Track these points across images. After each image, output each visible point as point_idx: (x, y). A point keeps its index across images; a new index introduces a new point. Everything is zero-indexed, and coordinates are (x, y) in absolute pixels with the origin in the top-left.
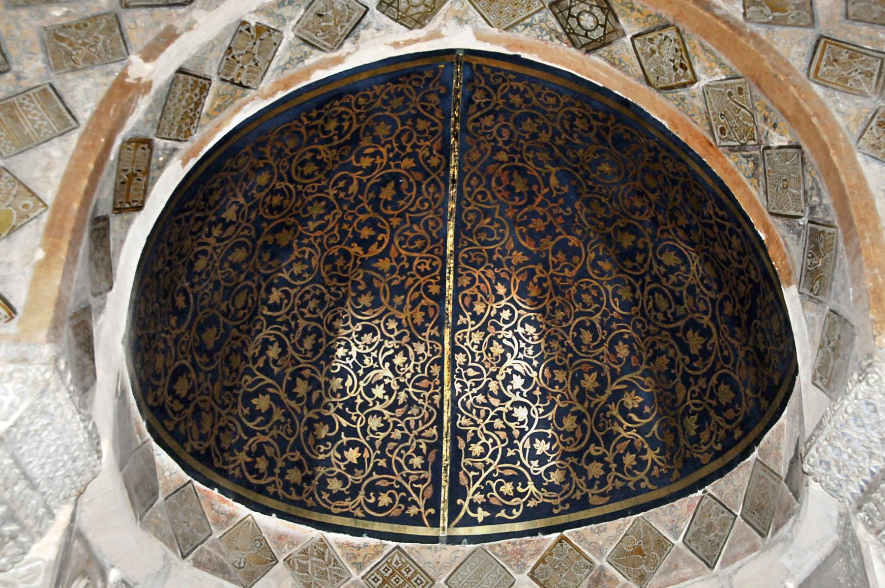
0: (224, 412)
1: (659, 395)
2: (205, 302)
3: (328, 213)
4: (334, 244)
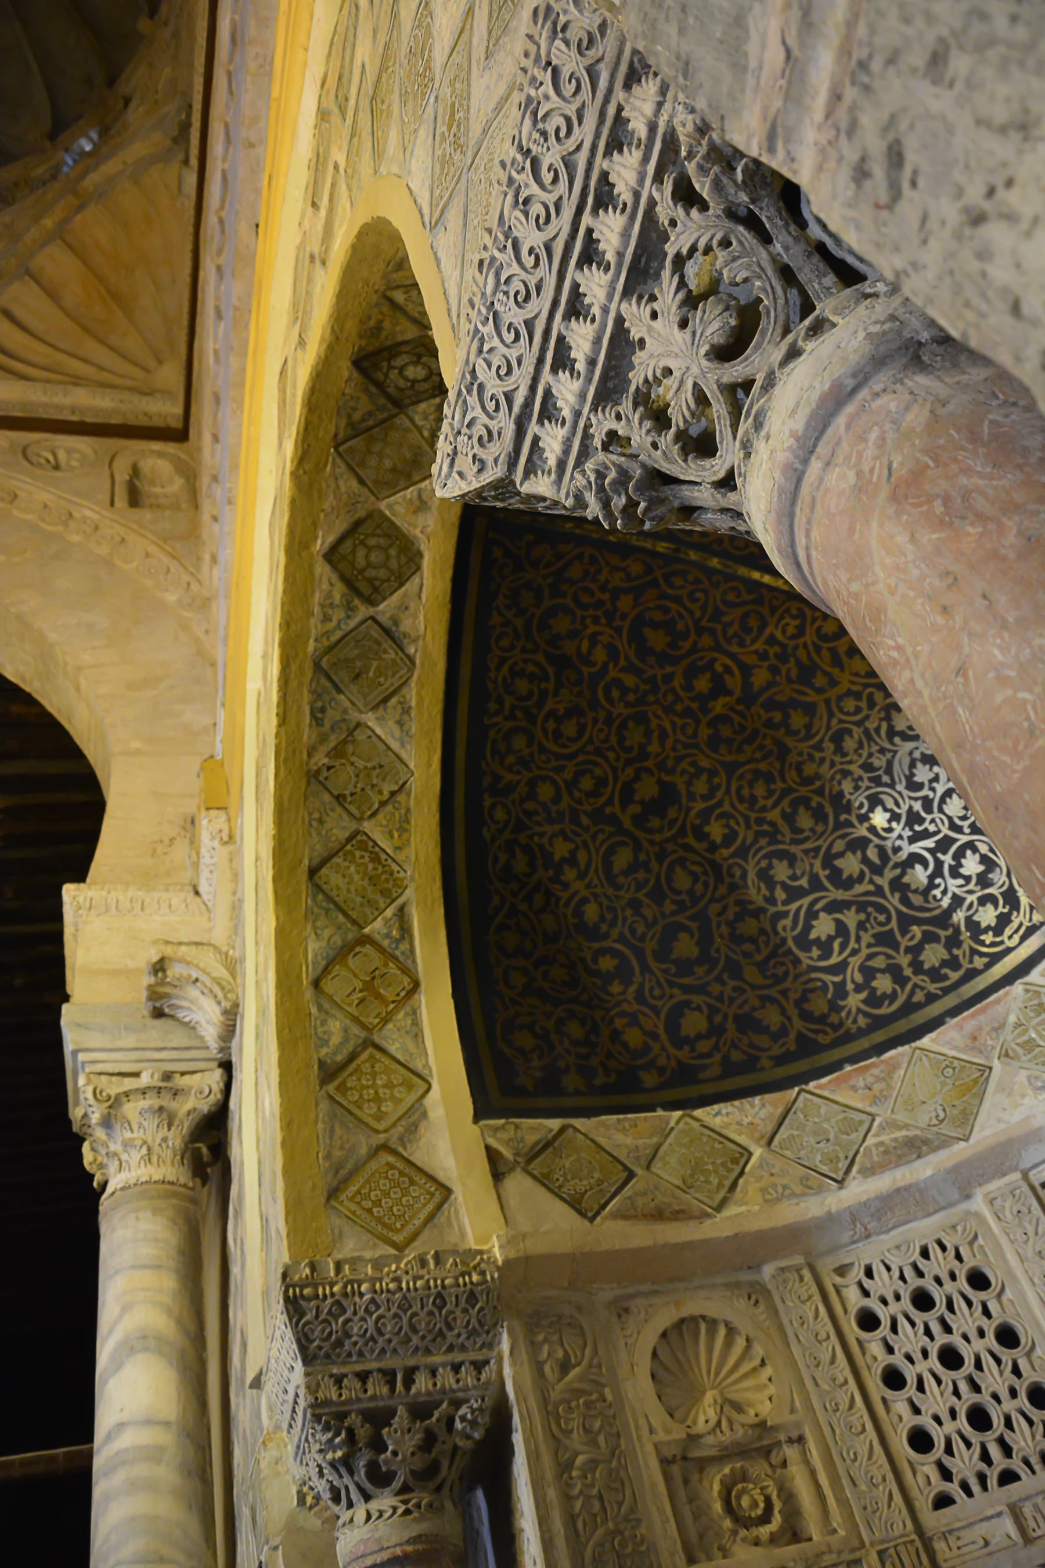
2: (640, 929)
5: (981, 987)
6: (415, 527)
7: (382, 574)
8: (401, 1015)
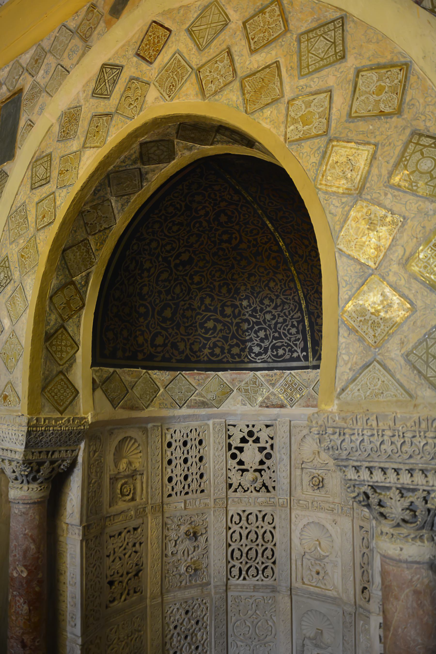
0: (190, 337)
2: (158, 301)
5: (243, 367)
6: (180, 151)
8: (75, 317)
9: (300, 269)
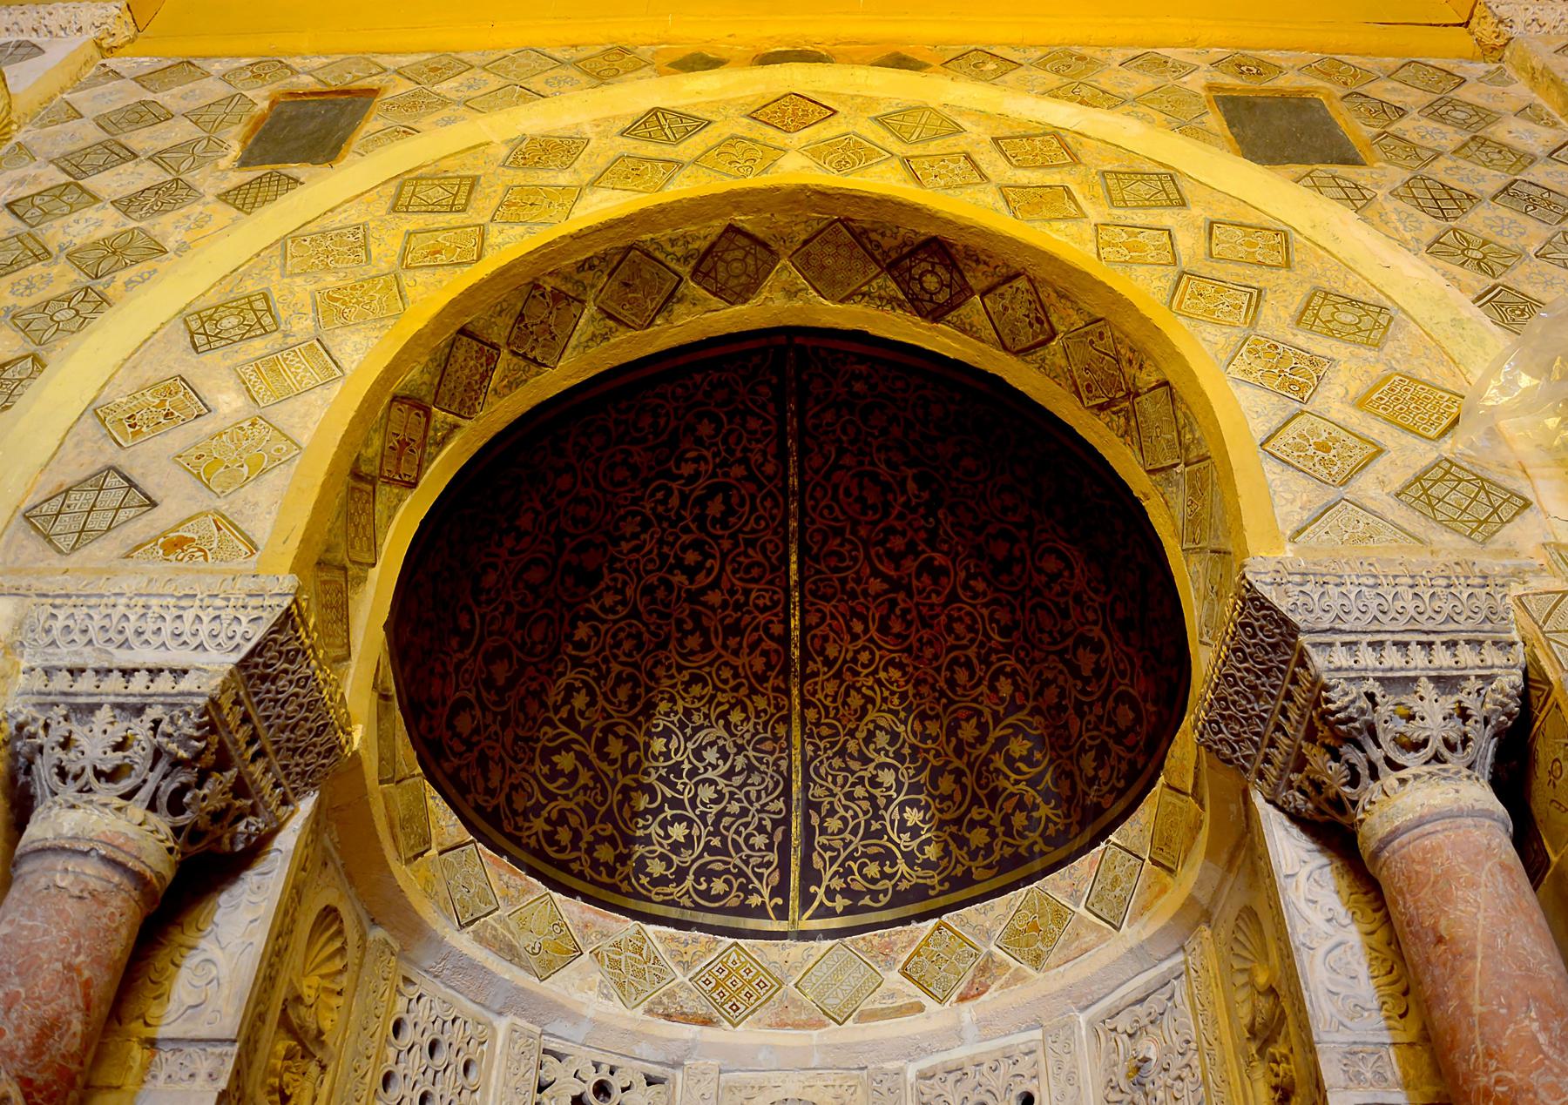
0: (517, 767)
1: (1050, 735)
2: (494, 627)
3: (645, 530)
4: (651, 572)
7: (722, 276)
9: (813, 695)
